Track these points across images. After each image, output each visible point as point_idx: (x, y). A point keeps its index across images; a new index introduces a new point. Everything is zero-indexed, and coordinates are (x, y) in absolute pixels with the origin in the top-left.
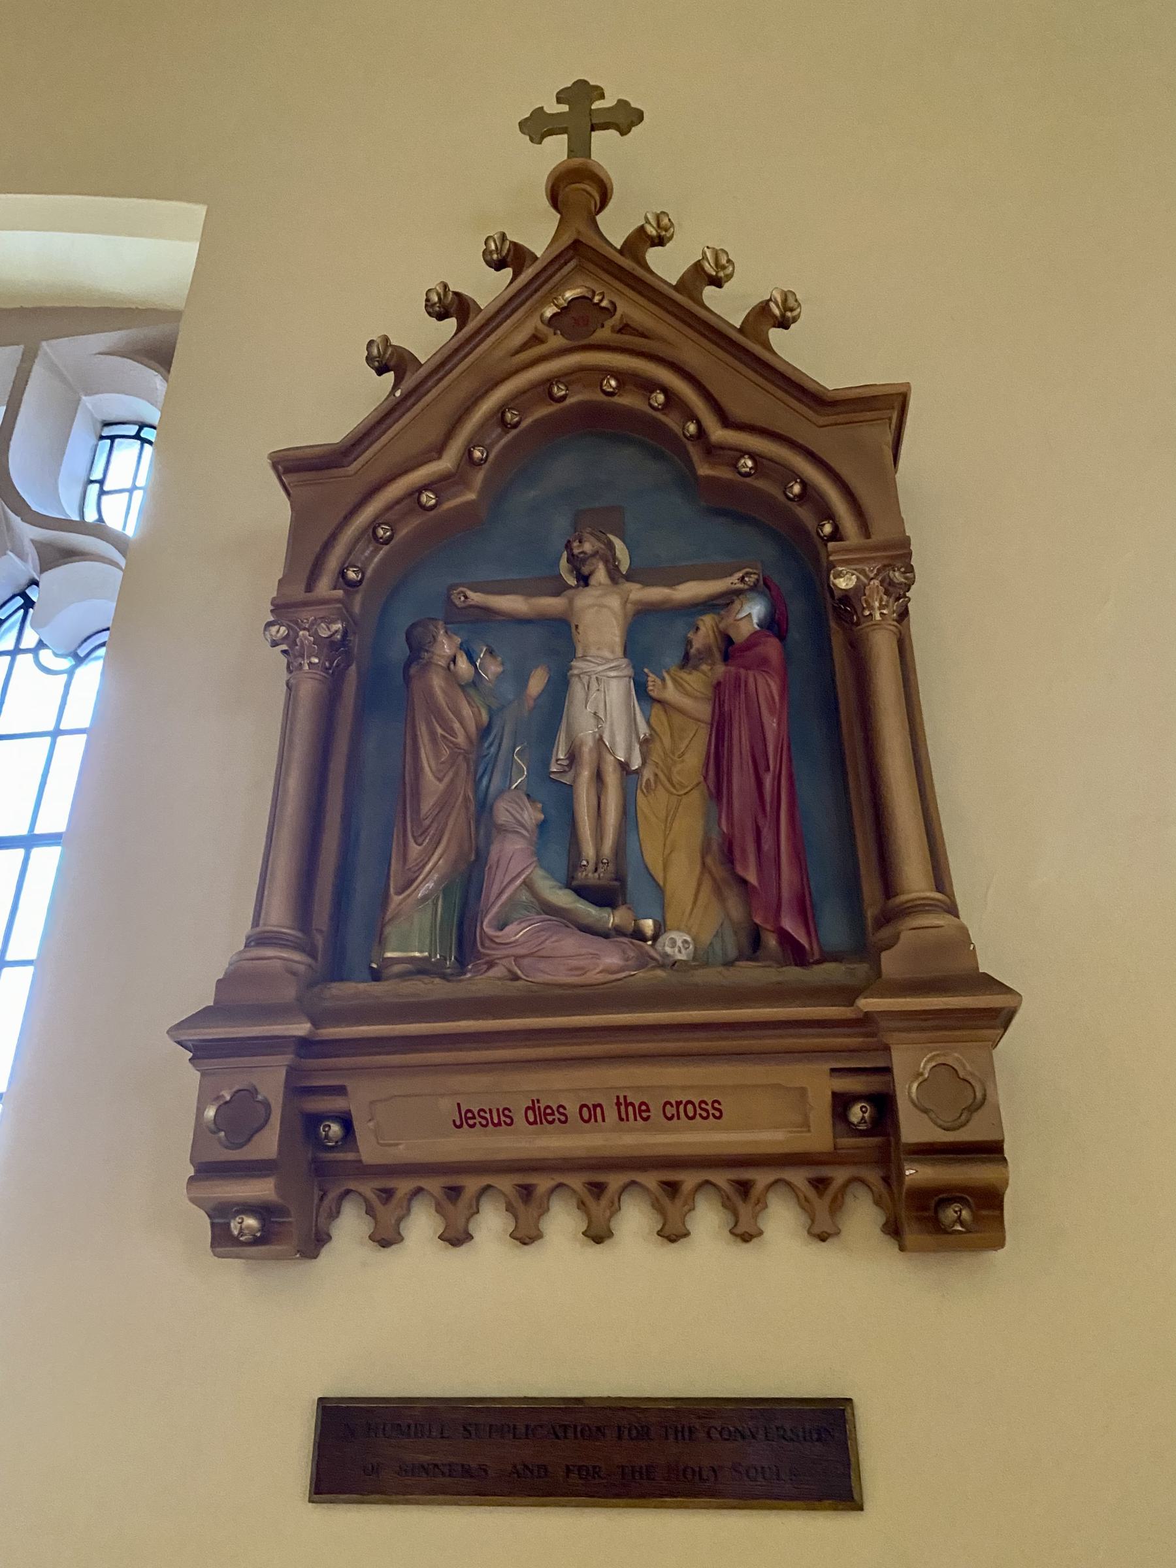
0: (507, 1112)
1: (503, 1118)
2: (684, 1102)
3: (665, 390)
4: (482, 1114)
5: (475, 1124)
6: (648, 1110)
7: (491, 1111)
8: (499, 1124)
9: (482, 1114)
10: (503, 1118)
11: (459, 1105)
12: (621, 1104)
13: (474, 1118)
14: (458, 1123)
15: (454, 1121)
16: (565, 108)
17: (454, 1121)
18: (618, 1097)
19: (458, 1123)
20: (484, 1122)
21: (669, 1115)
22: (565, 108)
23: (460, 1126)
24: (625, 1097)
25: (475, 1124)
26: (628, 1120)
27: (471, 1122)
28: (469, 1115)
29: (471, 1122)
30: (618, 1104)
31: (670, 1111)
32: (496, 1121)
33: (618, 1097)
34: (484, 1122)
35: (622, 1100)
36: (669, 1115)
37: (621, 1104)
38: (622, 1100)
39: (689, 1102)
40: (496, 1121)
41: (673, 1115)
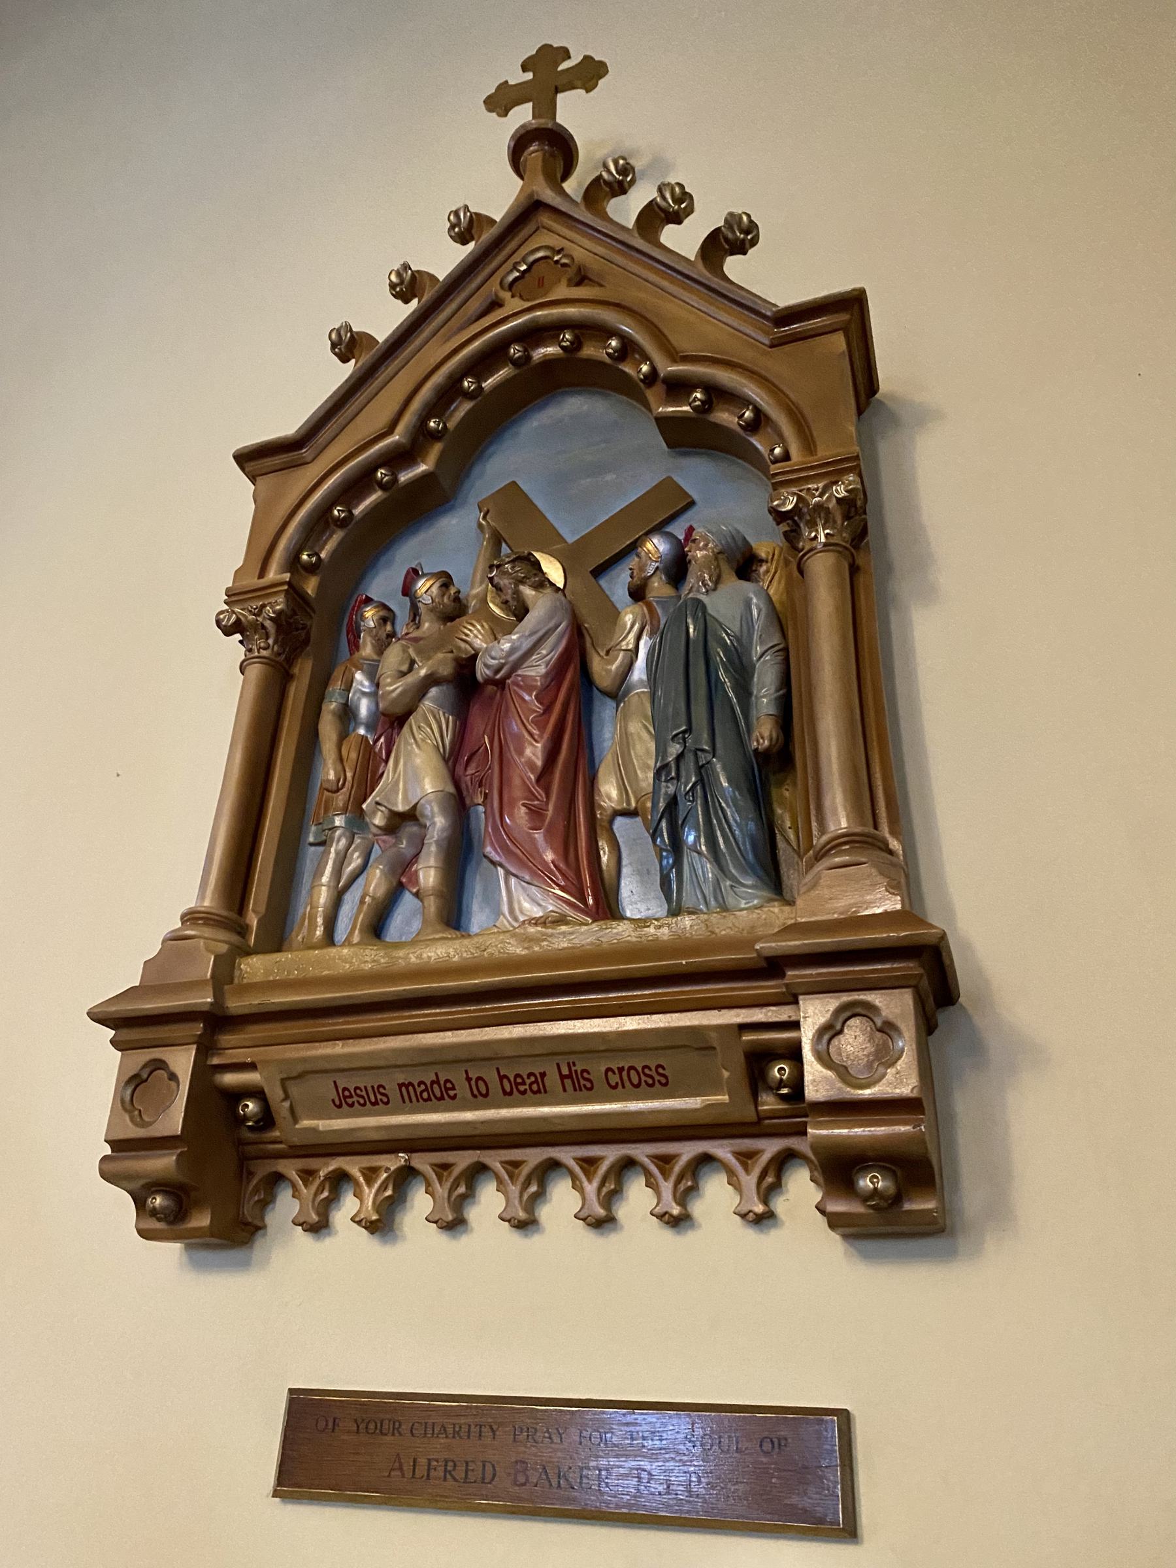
1: (379, 1097)
2: (626, 1068)
5: (353, 1103)
10: (379, 1097)
11: (335, 1082)
14: (337, 1102)
15: (333, 1101)
16: (529, 76)
17: (333, 1101)
19: (337, 1102)
21: (614, 1084)
22: (529, 76)
25: (353, 1103)
27: (350, 1101)
28: (347, 1093)
31: (614, 1079)
32: (373, 1100)
36: (614, 1084)
39: (631, 1068)
40: (373, 1100)
41: (617, 1083)
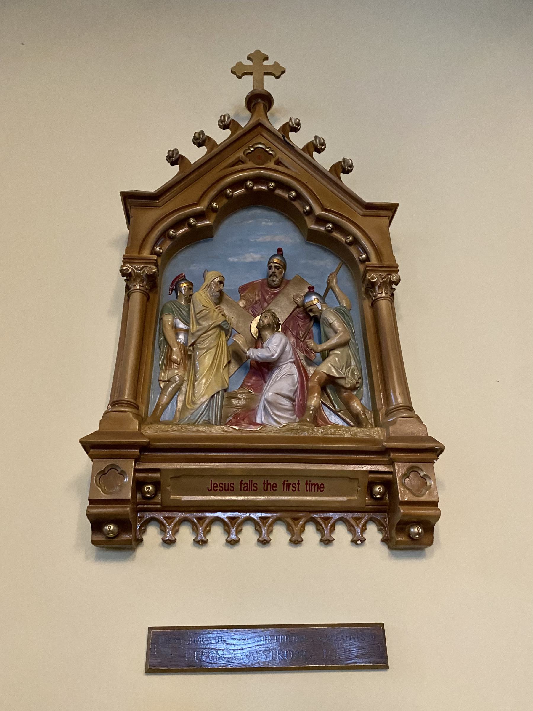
0: (232, 485)
3: (296, 191)
4: (221, 485)
5: (217, 489)
6: (276, 487)
7: (225, 484)
8: (228, 490)
9: (221, 485)
12: (265, 484)
13: (217, 487)
18: (264, 481)
20: (221, 489)
23: (210, 490)
24: (267, 481)
25: (217, 489)
26: (267, 491)
27: (215, 489)
28: (215, 485)
29: (215, 489)
30: (264, 484)
32: (226, 489)
33: (264, 481)
34: (221, 489)
35: (266, 482)
37: (265, 484)
38: (266, 482)
40: (226, 489)
